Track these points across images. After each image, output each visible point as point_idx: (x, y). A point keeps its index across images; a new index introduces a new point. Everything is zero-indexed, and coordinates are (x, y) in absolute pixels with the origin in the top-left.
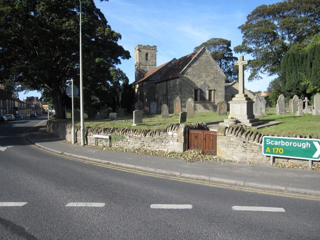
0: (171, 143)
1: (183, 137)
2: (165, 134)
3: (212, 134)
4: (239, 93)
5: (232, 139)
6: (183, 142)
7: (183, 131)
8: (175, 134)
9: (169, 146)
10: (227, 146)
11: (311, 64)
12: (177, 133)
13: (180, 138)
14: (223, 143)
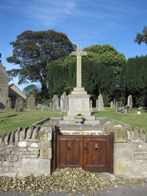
0: (25, 161)
1: (50, 150)
2: (11, 145)
3: (99, 140)
4: (77, 86)
5: (140, 146)
6: (50, 157)
7: (50, 138)
8: (35, 145)
9: (20, 166)
10: (133, 157)
11: (87, 70)
12: (37, 142)
13: (44, 151)
14: (126, 154)
